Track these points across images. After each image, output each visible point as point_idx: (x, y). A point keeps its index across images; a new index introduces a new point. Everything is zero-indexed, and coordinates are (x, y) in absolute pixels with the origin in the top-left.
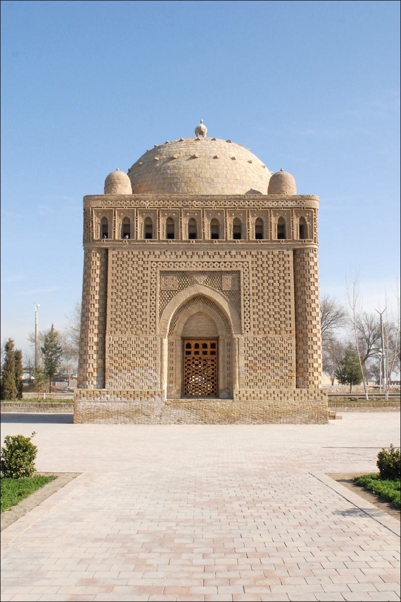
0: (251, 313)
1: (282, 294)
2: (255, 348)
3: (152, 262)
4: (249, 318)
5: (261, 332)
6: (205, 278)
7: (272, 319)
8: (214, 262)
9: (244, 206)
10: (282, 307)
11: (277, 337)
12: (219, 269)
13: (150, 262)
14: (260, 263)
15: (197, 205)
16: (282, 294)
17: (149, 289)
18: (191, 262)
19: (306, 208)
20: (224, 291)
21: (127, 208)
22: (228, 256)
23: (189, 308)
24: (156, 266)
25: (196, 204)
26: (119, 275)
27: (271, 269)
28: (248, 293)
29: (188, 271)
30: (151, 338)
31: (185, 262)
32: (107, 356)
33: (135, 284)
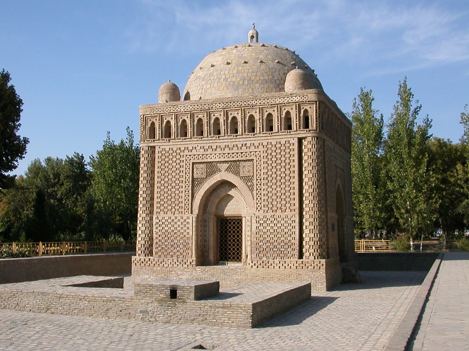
0: (262, 195)
1: (287, 178)
2: (265, 225)
3: (187, 155)
4: (261, 199)
5: (270, 211)
6: (226, 165)
7: (279, 200)
8: (233, 153)
9: (256, 104)
10: (287, 189)
11: (283, 215)
12: (237, 159)
13: (185, 156)
14: (269, 152)
15: (220, 107)
16: (287, 178)
17: (184, 177)
18: (215, 154)
19: (308, 102)
20: (242, 177)
21: (168, 114)
22: (244, 148)
23: (218, 192)
24: (189, 158)
25: (219, 106)
26: (163, 167)
27: (279, 156)
28: (260, 178)
29: (214, 162)
30: (185, 218)
31: (211, 154)
32: (154, 232)
33: (174, 174)
